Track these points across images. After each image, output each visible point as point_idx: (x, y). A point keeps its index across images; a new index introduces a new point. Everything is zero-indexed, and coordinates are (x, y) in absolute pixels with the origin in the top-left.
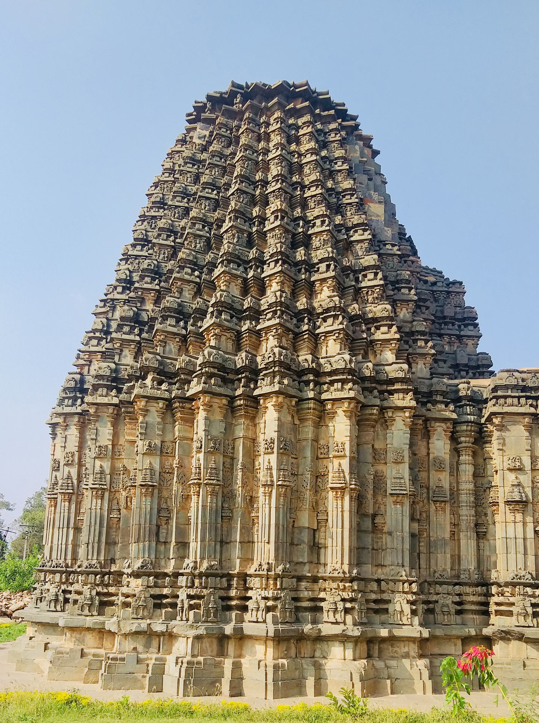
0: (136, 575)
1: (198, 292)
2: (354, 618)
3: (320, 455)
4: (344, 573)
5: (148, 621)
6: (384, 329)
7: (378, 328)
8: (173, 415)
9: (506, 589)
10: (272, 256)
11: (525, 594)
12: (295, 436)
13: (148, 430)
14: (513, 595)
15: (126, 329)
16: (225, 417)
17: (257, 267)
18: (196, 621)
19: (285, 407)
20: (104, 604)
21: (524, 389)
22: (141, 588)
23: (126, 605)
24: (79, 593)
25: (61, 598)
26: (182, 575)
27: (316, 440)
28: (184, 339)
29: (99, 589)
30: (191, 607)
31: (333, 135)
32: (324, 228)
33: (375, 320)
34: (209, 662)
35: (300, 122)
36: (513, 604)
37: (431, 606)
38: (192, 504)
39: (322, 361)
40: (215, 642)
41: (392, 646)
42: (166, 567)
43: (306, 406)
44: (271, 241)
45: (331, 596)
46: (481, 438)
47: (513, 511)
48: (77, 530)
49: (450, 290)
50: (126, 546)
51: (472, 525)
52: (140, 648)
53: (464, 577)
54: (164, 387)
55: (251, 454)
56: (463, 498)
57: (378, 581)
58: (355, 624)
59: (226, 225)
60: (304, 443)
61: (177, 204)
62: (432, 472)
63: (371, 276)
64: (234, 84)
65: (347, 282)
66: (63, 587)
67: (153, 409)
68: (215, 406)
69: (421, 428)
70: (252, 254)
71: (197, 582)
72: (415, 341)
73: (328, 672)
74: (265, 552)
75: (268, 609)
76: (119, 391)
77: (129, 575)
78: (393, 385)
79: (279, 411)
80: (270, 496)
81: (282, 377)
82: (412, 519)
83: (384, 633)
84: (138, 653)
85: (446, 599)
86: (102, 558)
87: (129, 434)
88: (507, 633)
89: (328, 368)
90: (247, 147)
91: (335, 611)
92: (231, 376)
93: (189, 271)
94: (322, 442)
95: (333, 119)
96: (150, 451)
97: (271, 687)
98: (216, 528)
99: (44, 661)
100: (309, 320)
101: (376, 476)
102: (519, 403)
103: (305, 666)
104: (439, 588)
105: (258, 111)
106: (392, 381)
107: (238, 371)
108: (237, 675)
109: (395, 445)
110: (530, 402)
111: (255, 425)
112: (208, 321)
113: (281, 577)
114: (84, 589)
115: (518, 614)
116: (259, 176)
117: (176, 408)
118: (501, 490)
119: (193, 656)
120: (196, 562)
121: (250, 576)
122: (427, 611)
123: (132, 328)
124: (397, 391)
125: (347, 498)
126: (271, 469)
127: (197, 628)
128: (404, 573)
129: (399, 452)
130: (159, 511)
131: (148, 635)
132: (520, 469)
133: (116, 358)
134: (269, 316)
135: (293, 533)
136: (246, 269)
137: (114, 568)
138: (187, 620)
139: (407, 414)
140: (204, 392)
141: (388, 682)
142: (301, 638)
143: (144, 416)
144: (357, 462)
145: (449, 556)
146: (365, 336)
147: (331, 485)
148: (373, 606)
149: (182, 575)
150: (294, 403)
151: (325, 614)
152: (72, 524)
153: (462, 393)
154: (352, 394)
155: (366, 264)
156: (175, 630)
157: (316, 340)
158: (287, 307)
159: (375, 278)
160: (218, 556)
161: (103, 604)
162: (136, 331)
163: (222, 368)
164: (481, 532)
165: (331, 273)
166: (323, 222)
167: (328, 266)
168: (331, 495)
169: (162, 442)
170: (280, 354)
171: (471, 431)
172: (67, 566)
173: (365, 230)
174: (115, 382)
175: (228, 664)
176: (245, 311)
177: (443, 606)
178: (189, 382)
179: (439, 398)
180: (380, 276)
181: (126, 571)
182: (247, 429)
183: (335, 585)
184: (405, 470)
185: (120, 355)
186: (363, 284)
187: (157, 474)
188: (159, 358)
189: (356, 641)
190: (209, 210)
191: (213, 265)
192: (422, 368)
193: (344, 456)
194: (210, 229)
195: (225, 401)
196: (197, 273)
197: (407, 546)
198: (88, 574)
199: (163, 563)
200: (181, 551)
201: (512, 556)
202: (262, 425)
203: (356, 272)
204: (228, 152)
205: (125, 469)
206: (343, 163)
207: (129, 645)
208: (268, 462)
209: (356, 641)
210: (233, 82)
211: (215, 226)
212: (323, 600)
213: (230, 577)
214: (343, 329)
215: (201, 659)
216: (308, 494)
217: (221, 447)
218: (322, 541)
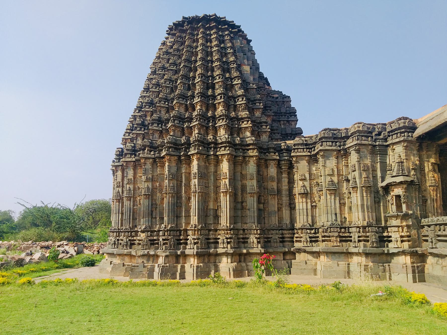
0: (143, 232)
1: (168, 112)
2: (231, 246)
3: (217, 179)
4: (227, 227)
5: (148, 250)
6: (245, 122)
7: (243, 122)
8: (157, 164)
9: (299, 231)
10: (197, 94)
11: (307, 233)
12: (207, 171)
13: (146, 172)
14: (302, 233)
15: (138, 129)
17: (191, 99)
18: (166, 250)
19: (201, 159)
20: (131, 244)
21: (306, 145)
22: (145, 237)
23: (139, 244)
24: (122, 240)
25: (117, 243)
26: (161, 231)
27: (216, 172)
28: (161, 132)
29: (130, 238)
30: (164, 244)
31: (226, 37)
32: (220, 80)
33: (242, 119)
34: (171, 266)
35: (212, 32)
36: (302, 237)
37: (269, 239)
38: (165, 202)
39: (218, 138)
40: (174, 258)
41: (250, 257)
42: (156, 228)
43: (210, 158)
44: (198, 87)
45: (222, 237)
46: (291, 167)
47: (302, 197)
48: (122, 214)
50: (140, 220)
51: (288, 204)
52: (145, 262)
53: (284, 227)
54: (152, 153)
55: (188, 180)
56: (284, 192)
57: (244, 230)
58: (231, 248)
59: (179, 81)
60: (211, 173)
61: (160, 73)
62: (269, 182)
63: (240, 99)
64: (184, 18)
65: (230, 102)
66: (117, 238)
67: (148, 163)
68: (172, 160)
69: (262, 164)
70: (190, 93)
71: (166, 233)
72: (262, 126)
73: (220, 268)
74: (194, 220)
75: (195, 243)
76: (135, 155)
78: (249, 146)
79: (198, 161)
80: (195, 197)
81: (199, 147)
82: (259, 202)
83: (245, 251)
84: (144, 263)
85: (275, 236)
86: (131, 225)
87: (140, 173)
88: (299, 249)
89: (220, 141)
90: (189, 46)
91: (223, 243)
92: (180, 147)
93: (163, 102)
94: (218, 173)
95: (227, 29)
96: (147, 180)
97: (195, 275)
98: (174, 211)
99: (109, 268)
100: (213, 121)
101: (242, 186)
102: (303, 151)
103: (211, 266)
104: (272, 232)
105: (193, 29)
106: (249, 145)
107: (182, 145)
108: (183, 271)
109: (250, 172)
110: (308, 150)
111: (190, 167)
112: (170, 124)
113: (201, 230)
114: (124, 238)
115: (304, 241)
116: (193, 58)
117: (157, 161)
118: (297, 188)
119: (165, 264)
120: (166, 225)
121: (188, 230)
122: (266, 242)
123: (141, 128)
124: (251, 149)
125: (228, 196)
126: (195, 185)
127: (166, 252)
128: (254, 226)
129: (252, 175)
130: (152, 205)
131: (148, 256)
132: (305, 180)
133: (135, 141)
134: (195, 120)
135: (207, 211)
136: (187, 100)
137: (136, 229)
138: (163, 249)
139: (255, 159)
140: (167, 154)
141: (247, 271)
142: (210, 255)
143: (144, 166)
144: (233, 180)
145: (277, 218)
146: (237, 126)
147: (221, 191)
148: (241, 240)
149: (161, 231)
150: (205, 157)
151: (220, 244)
152: (120, 212)
153: (283, 147)
154: (228, 152)
155: (239, 94)
156: (158, 254)
157: (216, 130)
158: (203, 116)
159: (242, 100)
160: (175, 222)
161: (132, 244)
162: (143, 129)
163: (175, 144)
164: (292, 207)
165: (222, 100)
166: (219, 77)
167: (221, 97)
168: (222, 194)
169: (152, 176)
170: (198, 137)
171: (286, 164)
172: (119, 229)
173: (238, 79)
174: (134, 151)
175: (179, 266)
176: (186, 118)
177: (274, 239)
178: (162, 150)
179: (272, 150)
180: (244, 99)
181: (140, 230)
182: (186, 169)
183: (223, 232)
184: (255, 182)
185: (136, 140)
186: (237, 103)
187: (151, 190)
188: (150, 141)
189: (232, 255)
190: (173, 75)
191: (173, 99)
192: (265, 138)
193: (227, 178)
194: (173, 83)
196: (167, 103)
198: (125, 232)
199: (154, 226)
200: (161, 221)
201: (301, 217)
202: (192, 167)
203: (235, 98)
204: (181, 48)
205: (139, 188)
206: (231, 49)
207: (140, 260)
208: (195, 182)
209: (232, 255)
210: (183, 17)
211: (174, 82)
212: (219, 239)
213: (180, 231)
214: (226, 124)
215: (168, 265)
216: (212, 195)
217: (176, 177)
218: (219, 214)
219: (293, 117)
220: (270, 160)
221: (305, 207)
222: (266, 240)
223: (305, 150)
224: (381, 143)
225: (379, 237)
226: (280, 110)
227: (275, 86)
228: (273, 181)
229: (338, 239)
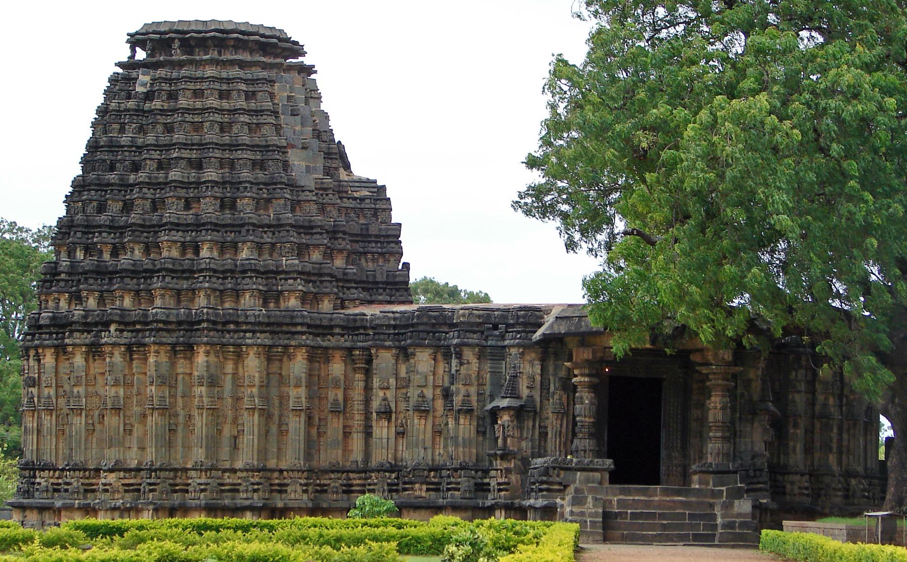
16: (170, 358)
23: (106, 491)
49: (377, 206)
57: (281, 471)
77: (105, 471)
125: (256, 416)
129: (299, 379)
179: (337, 330)
184: (302, 391)
193: (254, 386)
195: (169, 348)
197: (302, 446)
219: (392, 245)
220: (333, 348)
221: (385, 435)
222: (319, 488)
225: (476, 484)
226: (367, 229)
227: (362, 165)
228: (337, 387)
229: (424, 487)
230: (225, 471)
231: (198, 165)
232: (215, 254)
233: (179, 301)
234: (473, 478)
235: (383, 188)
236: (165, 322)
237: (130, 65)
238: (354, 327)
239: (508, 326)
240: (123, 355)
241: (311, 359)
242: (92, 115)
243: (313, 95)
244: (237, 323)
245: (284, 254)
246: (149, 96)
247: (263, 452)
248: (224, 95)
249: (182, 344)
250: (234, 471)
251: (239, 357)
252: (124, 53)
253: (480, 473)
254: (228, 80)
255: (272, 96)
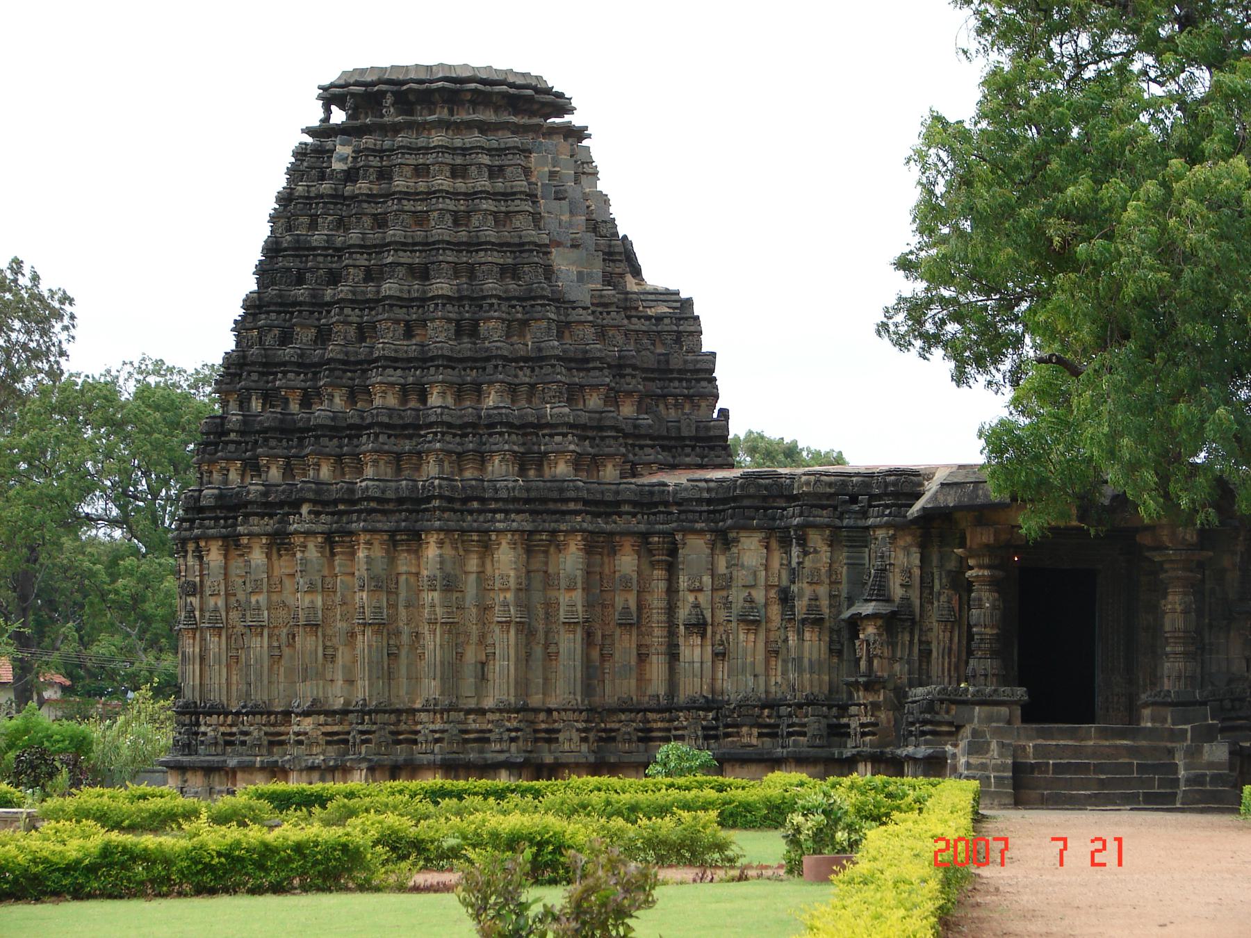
16: (387, 551)
23: (300, 743)
30: (364, 742)
49: (681, 328)
57: (549, 711)
71: (367, 717)
77: (297, 715)
125: (512, 632)
177: (625, 733)
179: (626, 508)
184: (578, 596)
195: (385, 537)
197: (579, 675)
219: (704, 384)
220: (622, 534)
221: (697, 658)
222: (604, 735)
223: (704, 515)
224: (852, 522)
225: (829, 726)
226: (667, 362)
227: (658, 271)
228: (627, 589)
229: (755, 731)
230: (469, 712)
231: (423, 273)
232: (450, 401)
233: (399, 470)
234: (825, 717)
235: (688, 303)
236: (379, 500)
237: (323, 132)
238: (651, 502)
239: (872, 497)
240: (321, 548)
241: (589, 550)
242: (271, 205)
243: (585, 169)
244: (482, 500)
245: (548, 399)
246: (351, 175)
247: (523, 685)
248: (457, 172)
249: (406, 531)
250: (482, 712)
251: (486, 548)
252: (314, 115)
253: (834, 709)
254: (464, 151)
255: (527, 172)
